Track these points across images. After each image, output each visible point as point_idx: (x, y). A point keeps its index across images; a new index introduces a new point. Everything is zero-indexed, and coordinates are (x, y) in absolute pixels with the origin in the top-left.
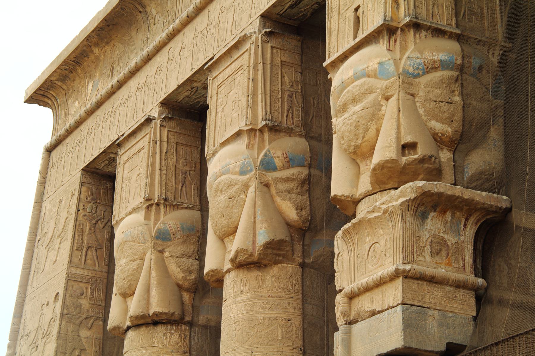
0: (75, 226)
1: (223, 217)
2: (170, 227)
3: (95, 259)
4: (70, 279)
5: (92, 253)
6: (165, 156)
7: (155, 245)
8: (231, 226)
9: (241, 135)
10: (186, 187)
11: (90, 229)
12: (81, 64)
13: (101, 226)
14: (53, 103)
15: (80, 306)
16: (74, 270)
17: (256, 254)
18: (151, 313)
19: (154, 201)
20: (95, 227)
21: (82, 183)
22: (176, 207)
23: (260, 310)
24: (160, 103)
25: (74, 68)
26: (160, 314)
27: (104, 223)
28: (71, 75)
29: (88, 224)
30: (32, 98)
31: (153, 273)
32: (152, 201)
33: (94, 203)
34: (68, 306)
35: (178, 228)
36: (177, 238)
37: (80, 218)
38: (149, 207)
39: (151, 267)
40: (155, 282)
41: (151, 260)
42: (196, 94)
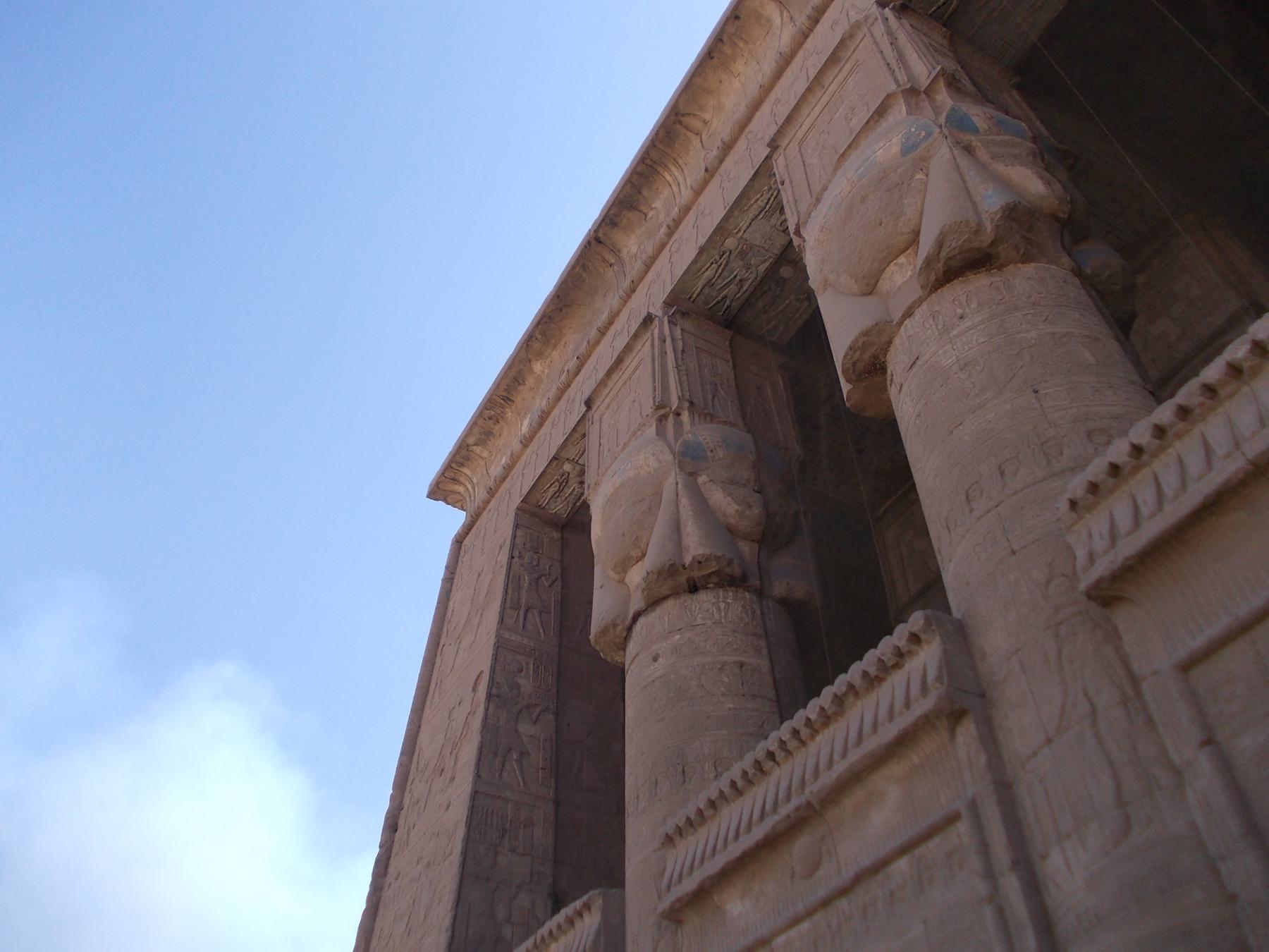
0: (508, 576)
1: (880, 225)
2: (704, 439)
3: (539, 626)
4: (500, 645)
5: (534, 617)
6: (682, 355)
7: (681, 466)
8: (904, 230)
9: (889, 110)
10: (719, 400)
11: (530, 584)
12: (513, 401)
13: (546, 584)
14: (468, 489)
15: (519, 687)
16: (507, 635)
17: (989, 227)
18: (688, 560)
19: (671, 409)
20: (537, 583)
21: (517, 524)
22: (708, 419)
23: (1024, 326)
24: (664, 302)
25: (502, 412)
26: (706, 560)
27: (550, 581)
28: (497, 427)
29: (526, 578)
30: (438, 488)
31: (684, 501)
32: (668, 409)
33: (534, 553)
34: (498, 683)
35: (718, 442)
36: (717, 458)
37: (515, 567)
38: (662, 419)
39: (677, 494)
40: (691, 513)
41: (677, 484)
42: (725, 274)
